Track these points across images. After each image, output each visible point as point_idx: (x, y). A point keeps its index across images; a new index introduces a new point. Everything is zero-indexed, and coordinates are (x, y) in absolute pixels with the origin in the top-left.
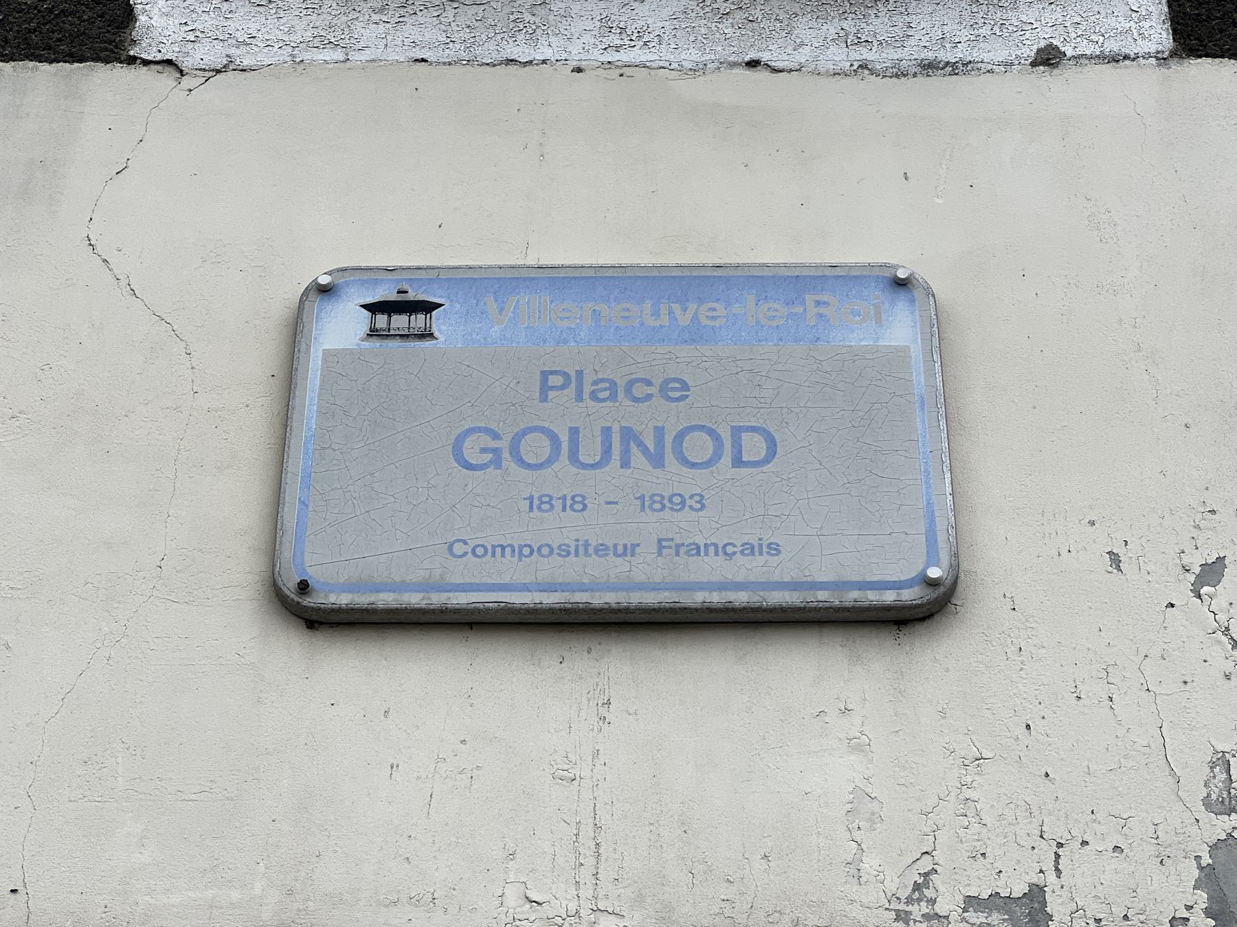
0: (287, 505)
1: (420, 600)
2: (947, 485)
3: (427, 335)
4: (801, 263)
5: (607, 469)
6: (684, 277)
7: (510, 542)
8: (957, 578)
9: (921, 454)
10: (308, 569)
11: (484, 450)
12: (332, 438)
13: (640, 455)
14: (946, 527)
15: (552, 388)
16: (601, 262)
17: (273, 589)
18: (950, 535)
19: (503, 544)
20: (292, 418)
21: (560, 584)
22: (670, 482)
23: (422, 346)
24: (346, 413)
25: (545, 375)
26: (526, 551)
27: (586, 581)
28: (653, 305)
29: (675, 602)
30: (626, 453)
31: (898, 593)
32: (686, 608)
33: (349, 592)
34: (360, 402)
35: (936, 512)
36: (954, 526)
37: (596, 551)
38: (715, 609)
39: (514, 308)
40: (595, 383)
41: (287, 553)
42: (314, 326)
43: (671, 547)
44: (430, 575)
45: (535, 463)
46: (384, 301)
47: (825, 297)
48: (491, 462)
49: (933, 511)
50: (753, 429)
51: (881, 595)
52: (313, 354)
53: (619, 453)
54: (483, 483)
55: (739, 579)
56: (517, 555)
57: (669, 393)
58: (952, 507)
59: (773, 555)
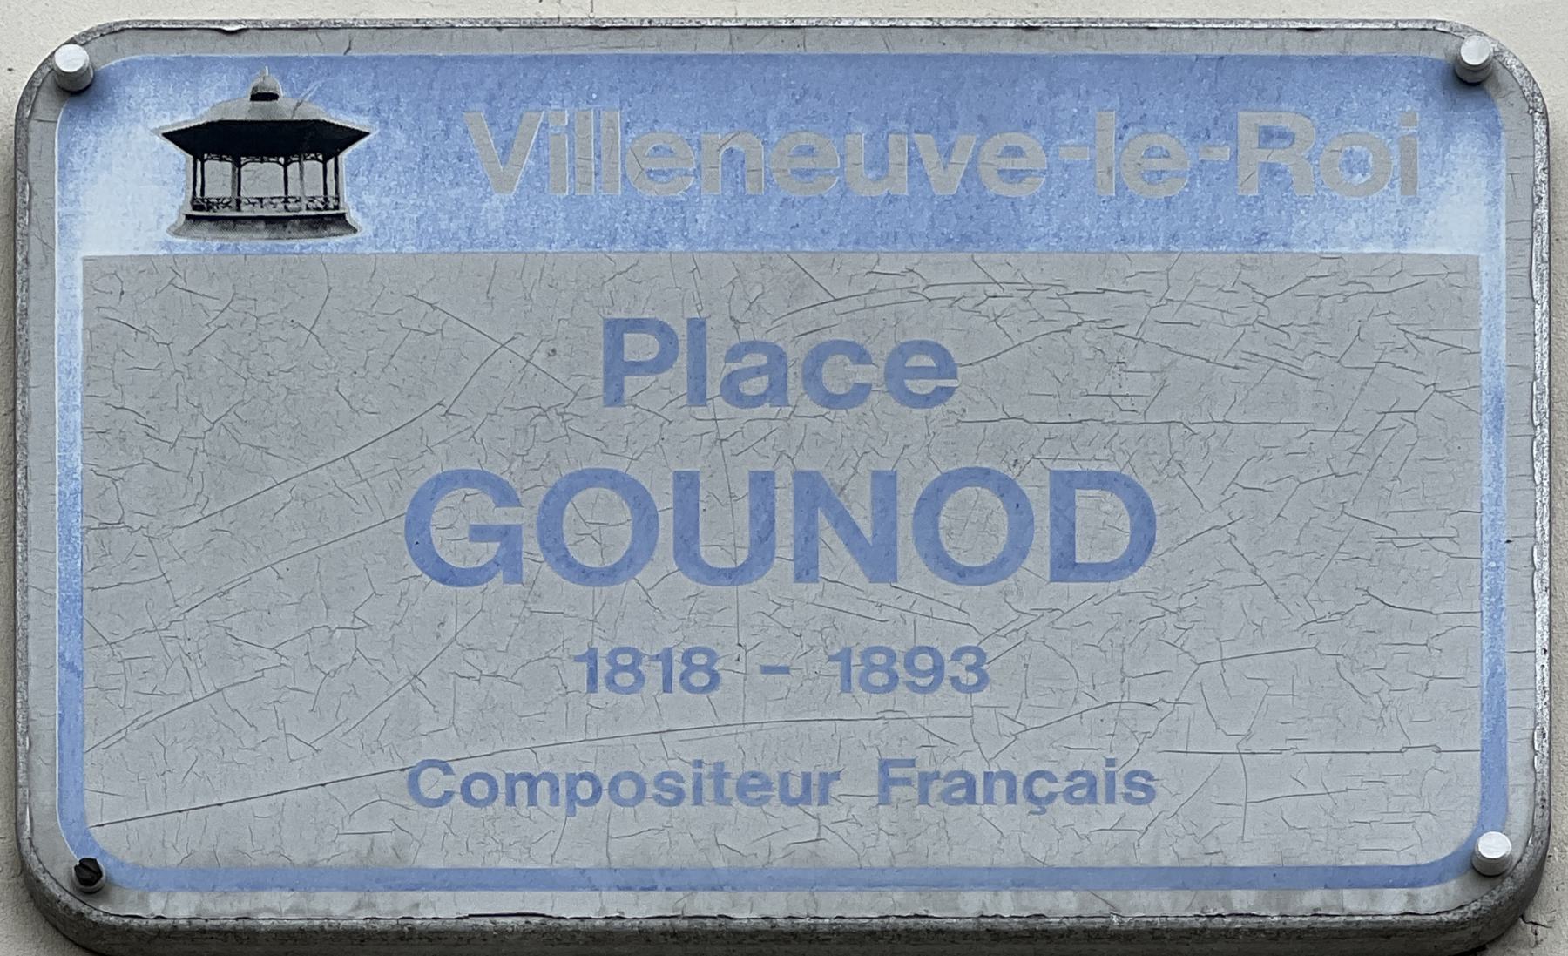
0: (33, 671)
1: (352, 910)
2: (1539, 628)
3: (329, 220)
4: (1231, 21)
5: (762, 583)
6: (946, 57)
7: (546, 768)
8: (1544, 858)
9: (1486, 546)
10: (97, 834)
11: (479, 533)
12: (123, 498)
13: (838, 544)
14: (1528, 734)
15: (636, 367)
16: (745, 13)
17: (21, 880)
18: (1536, 753)
19: (533, 772)
20: (25, 445)
21: (662, 871)
22: (909, 617)
23: (323, 249)
24: (150, 431)
25: (616, 330)
26: (584, 790)
27: (719, 863)
28: (870, 139)
29: (917, 916)
30: (807, 542)
31: (1409, 894)
32: (941, 931)
33: (193, 889)
34: (183, 404)
35: (1509, 694)
36: (1546, 731)
37: (742, 791)
38: (1006, 933)
39: (537, 143)
40: (734, 354)
41: (44, 796)
42: (57, 193)
43: (907, 782)
44: (371, 850)
45: (597, 566)
46: (221, 123)
47: (1286, 120)
48: (495, 562)
49: (1503, 693)
50: (1103, 481)
51: (1372, 900)
52: (61, 271)
53: (791, 541)
54: (480, 617)
55: (1061, 860)
56: (563, 799)
57: (908, 382)
58: (1546, 684)
59: (1139, 802)
